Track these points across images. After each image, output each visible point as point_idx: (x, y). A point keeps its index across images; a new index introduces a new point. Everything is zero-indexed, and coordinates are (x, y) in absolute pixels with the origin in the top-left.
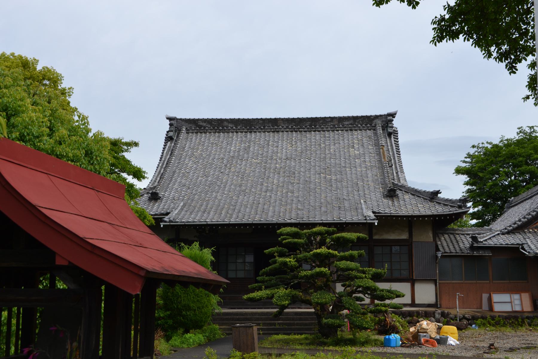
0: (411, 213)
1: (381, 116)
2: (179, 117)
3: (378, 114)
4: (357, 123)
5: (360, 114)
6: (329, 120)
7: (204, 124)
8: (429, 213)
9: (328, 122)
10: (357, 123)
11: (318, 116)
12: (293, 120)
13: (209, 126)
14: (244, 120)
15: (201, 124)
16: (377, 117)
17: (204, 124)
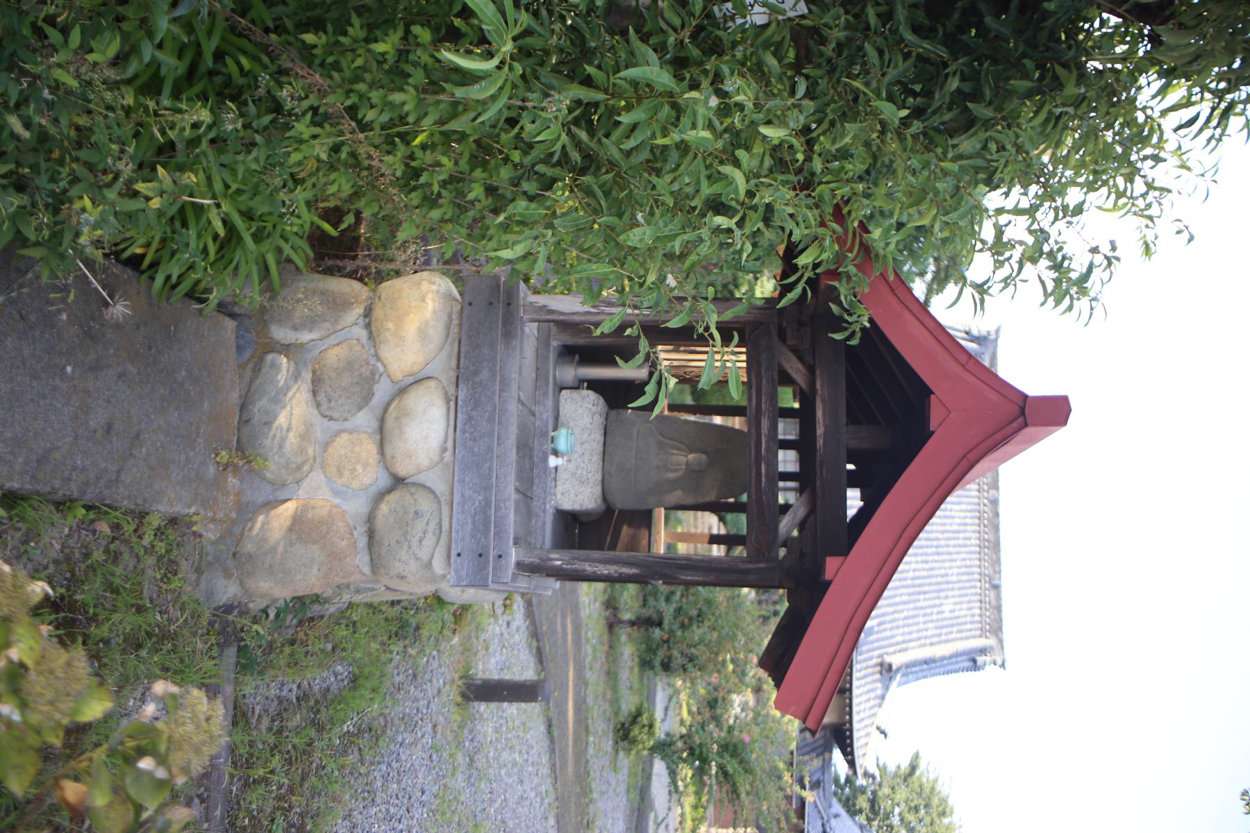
0: (855, 692)
5: (1004, 615)
8: (856, 726)
12: (997, 515)
16: (1001, 642)
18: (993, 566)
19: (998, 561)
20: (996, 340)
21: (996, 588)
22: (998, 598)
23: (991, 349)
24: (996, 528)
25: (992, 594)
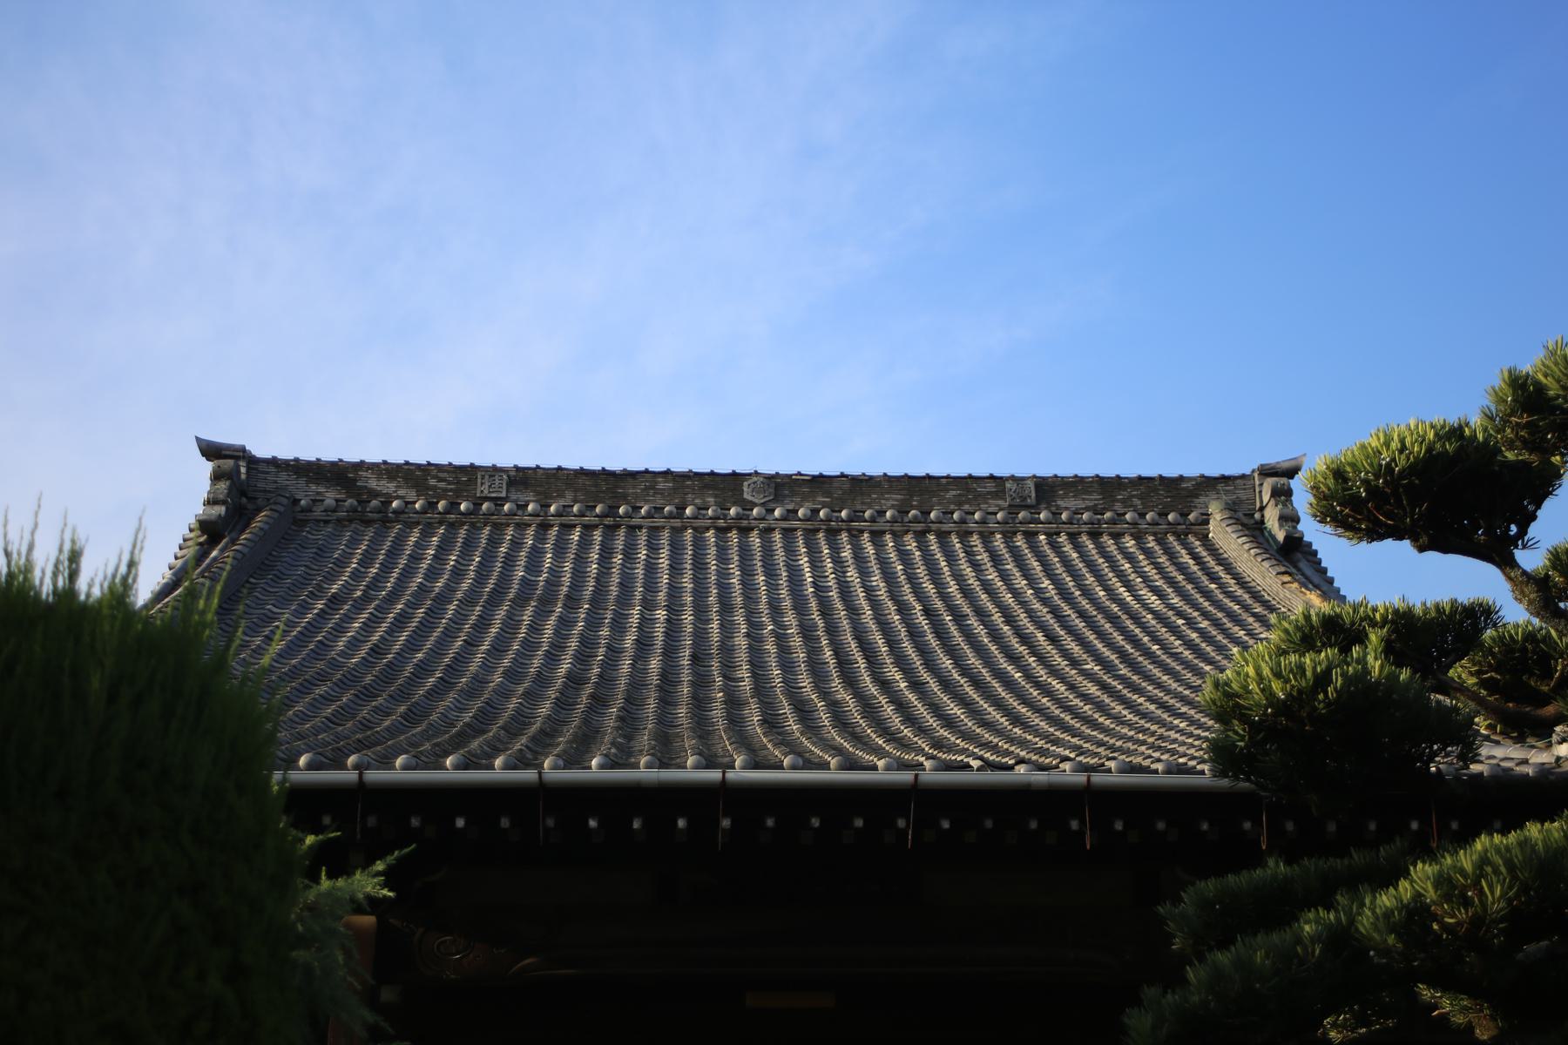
1: (1225, 479)
2: (261, 451)
3: (1214, 472)
4: (1118, 507)
5: (1129, 471)
6: (991, 487)
7: (389, 487)
9: (984, 497)
10: (1118, 507)
11: (938, 470)
12: (819, 481)
13: (411, 495)
14: (582, 472)
15: (373, 484)
16: (1208, 484)
17: (389, 487)
18: (979, 499)
19: (967, 486)
20: (253, 461)
21: (1047, 489)
22: (1077, 485)
23: (284, 475)
24: (860, 486)
25: (1068, 505)
